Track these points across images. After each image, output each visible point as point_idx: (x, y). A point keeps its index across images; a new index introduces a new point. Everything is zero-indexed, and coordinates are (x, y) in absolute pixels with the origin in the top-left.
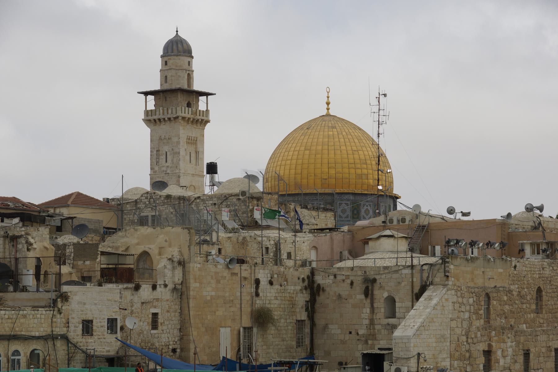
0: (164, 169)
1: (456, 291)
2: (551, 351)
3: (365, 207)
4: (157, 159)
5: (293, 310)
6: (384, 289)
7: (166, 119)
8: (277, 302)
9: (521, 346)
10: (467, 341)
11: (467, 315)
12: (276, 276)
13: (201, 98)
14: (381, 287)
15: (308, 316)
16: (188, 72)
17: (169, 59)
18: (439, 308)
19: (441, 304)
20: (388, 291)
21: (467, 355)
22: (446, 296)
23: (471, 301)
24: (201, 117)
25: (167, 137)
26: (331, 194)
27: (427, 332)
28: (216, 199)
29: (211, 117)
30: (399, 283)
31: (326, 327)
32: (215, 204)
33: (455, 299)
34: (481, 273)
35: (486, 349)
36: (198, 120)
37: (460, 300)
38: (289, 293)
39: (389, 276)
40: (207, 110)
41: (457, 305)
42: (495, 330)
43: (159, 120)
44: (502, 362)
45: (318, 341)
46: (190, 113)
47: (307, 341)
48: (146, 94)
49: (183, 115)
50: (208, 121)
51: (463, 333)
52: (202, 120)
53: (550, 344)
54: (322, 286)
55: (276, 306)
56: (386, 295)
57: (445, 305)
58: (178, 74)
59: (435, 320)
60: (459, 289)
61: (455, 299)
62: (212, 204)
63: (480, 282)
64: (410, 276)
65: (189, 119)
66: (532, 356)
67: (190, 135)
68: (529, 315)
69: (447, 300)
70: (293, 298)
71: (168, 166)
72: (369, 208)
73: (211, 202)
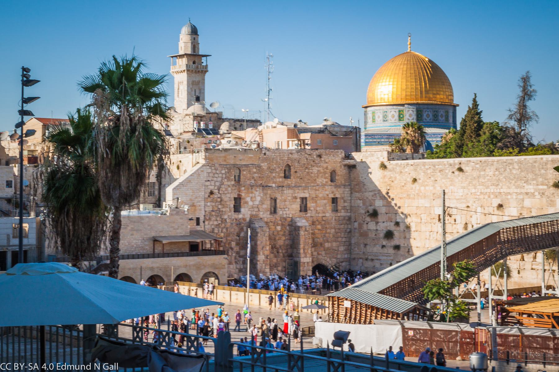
2: (296, 198)
3: (427, 113)
9: (268, 196)
10: (219, 193)
11: (220, 179)
13: (203, 58)
15: (157, 180)
18: (195, 175)
21: (219, 200)
22: (202, 169)
23: (223, 172)
26: (403, 105)
27: (185, 188)
29: (209, 69)
31: (164, 185)
33: (210, 171)
35: (236, 196)
36: (199, 71)
37: (214, 171)
40: (207, 65)
41: (211, 175)
42: (244, 186)
44: (251, 203)
45: (162, 193)
47: (156, 193)
48: (172, 57)
50: (207, 71)
51: (216, 188)
52: (202, 71)
53: (296, 195)
56: (184, 169)
61: (210, 171)
63: (232, 162)
66: (278, 201)
67: (194, 79)
68: (278, 180)
69: (202, 171)
72: (429, 113)
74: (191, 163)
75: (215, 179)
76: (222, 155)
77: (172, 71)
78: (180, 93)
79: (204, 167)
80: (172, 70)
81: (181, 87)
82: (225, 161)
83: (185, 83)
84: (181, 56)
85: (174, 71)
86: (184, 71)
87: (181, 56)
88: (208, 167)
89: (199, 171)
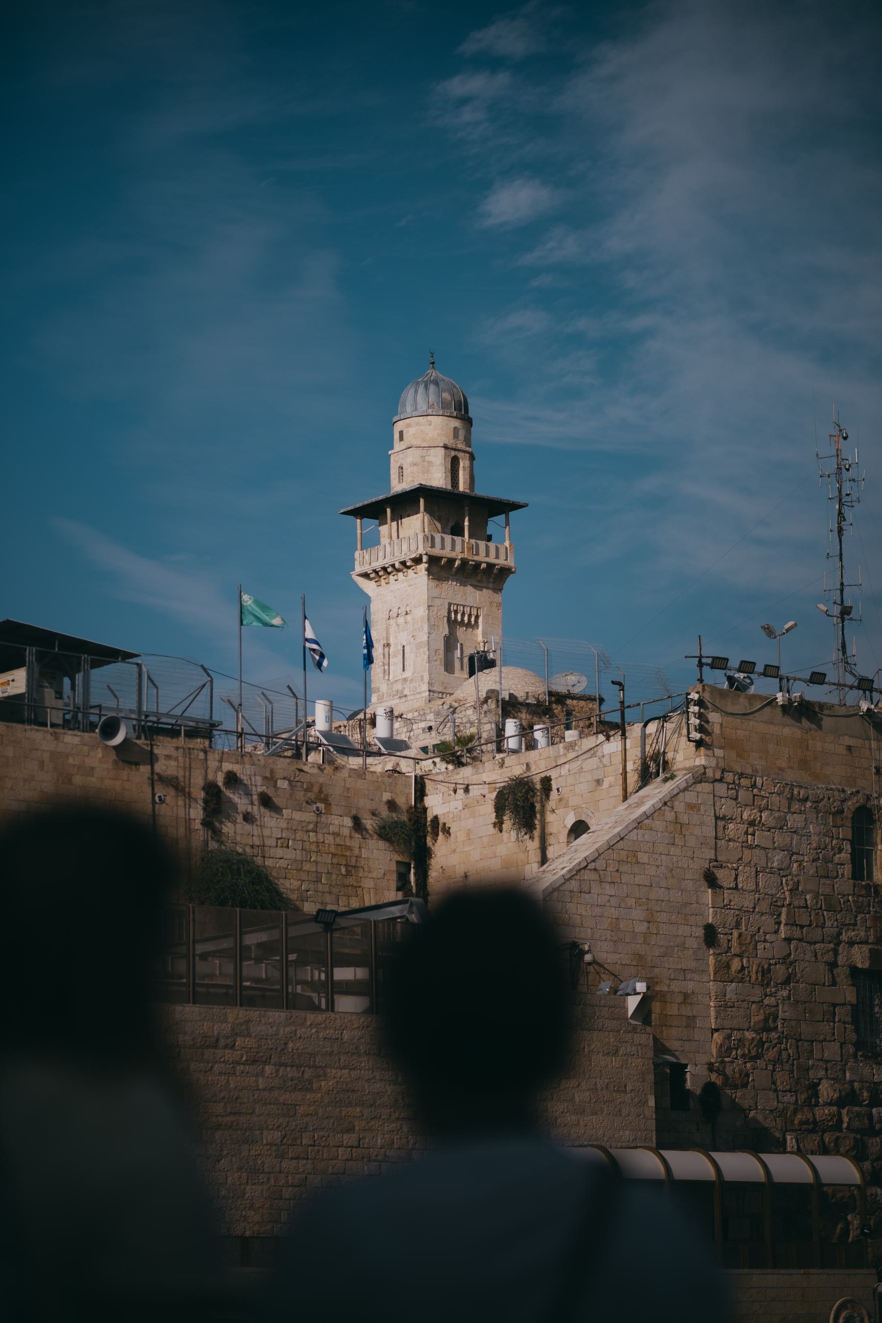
0: (399, 686)
1: (735, 786)
4: (384, 665)
5: (350, 881)
6: (566, 806)
7: (397, 565)
8: (289, 854)
12: (283, 784)
14: (561, 800)
16: (453, 453)
17: (409, 425)
18: (658, 824)
19: (670, 815)
20: (575, 808)
24: (492, 559)
25: (402, 611)
27: (609, 890)
28: (431, 717)
30: (599, 782)
32: (430, 728)
33: (726, 808)
34: (842, 750)
38: (336, 834)
39: (575, 765)
43: (384, 569)
46: (458, 548)
49: (437, 551)
52: (491, 566)
54: (441, 821)
55: (282, 863)
57: (684, 819)
58: (427, 458)
59: (643, 858)
60: (744, 782)
62: (424, 729)
64: (618, 759)
65: (451, 561)
69: (692, 807)
70: (350, 848)
71: (405, 680)
73: (423, 725)
74: (612, 781)
75: (758, 856)
76: (787, 731)
77: (358, 569)
78: (396, 661)
79: (706, 787)
80: (364, 561)
81: (399, 638)
82: (804, 764)
83: (421, 612)
84: (403, 504)
85: (367, 568)
86: (418, 561)
87: (403, 504)
88: (721, 789)
89: (679, 806)
